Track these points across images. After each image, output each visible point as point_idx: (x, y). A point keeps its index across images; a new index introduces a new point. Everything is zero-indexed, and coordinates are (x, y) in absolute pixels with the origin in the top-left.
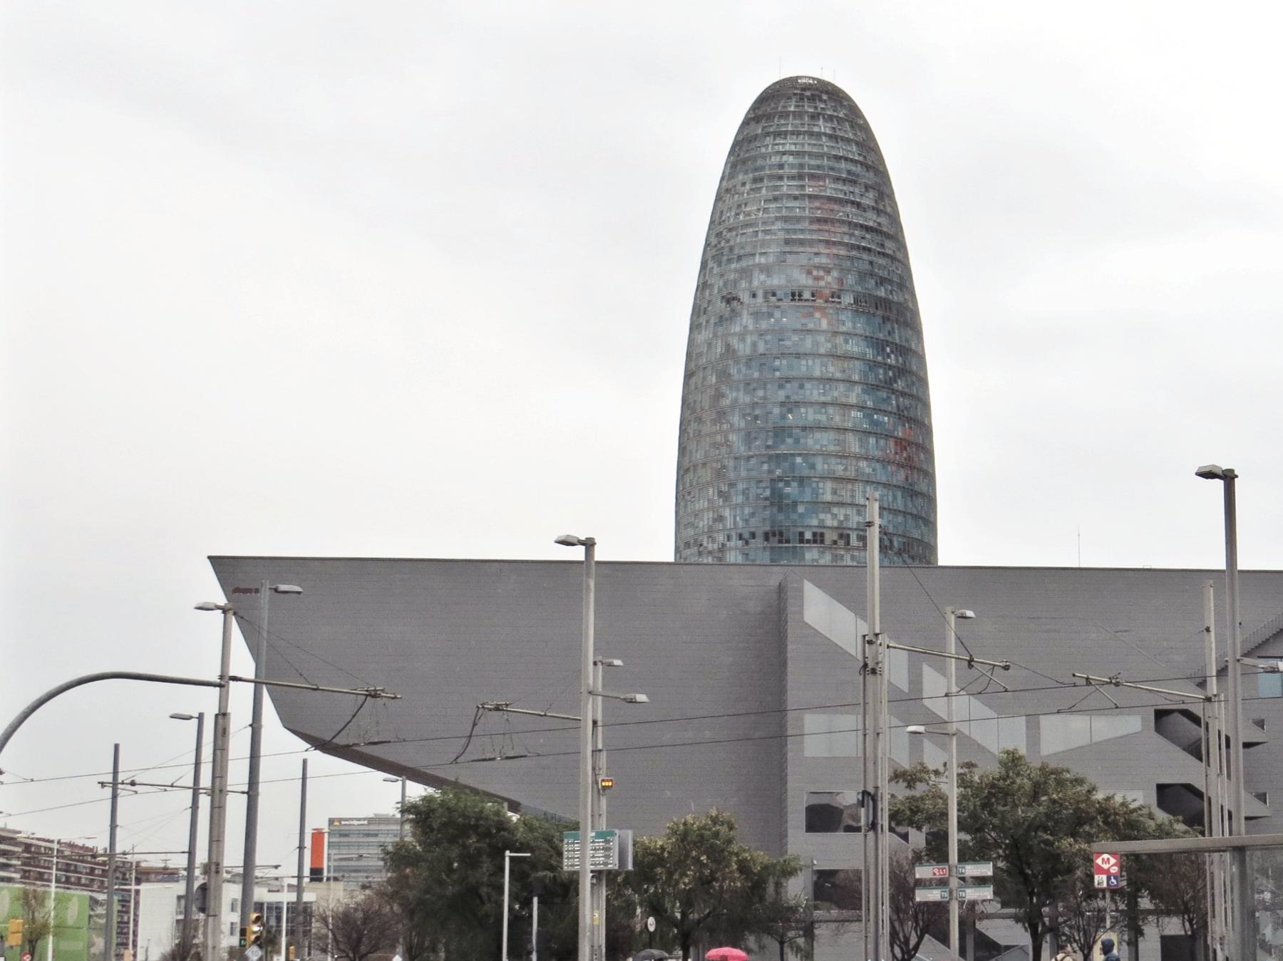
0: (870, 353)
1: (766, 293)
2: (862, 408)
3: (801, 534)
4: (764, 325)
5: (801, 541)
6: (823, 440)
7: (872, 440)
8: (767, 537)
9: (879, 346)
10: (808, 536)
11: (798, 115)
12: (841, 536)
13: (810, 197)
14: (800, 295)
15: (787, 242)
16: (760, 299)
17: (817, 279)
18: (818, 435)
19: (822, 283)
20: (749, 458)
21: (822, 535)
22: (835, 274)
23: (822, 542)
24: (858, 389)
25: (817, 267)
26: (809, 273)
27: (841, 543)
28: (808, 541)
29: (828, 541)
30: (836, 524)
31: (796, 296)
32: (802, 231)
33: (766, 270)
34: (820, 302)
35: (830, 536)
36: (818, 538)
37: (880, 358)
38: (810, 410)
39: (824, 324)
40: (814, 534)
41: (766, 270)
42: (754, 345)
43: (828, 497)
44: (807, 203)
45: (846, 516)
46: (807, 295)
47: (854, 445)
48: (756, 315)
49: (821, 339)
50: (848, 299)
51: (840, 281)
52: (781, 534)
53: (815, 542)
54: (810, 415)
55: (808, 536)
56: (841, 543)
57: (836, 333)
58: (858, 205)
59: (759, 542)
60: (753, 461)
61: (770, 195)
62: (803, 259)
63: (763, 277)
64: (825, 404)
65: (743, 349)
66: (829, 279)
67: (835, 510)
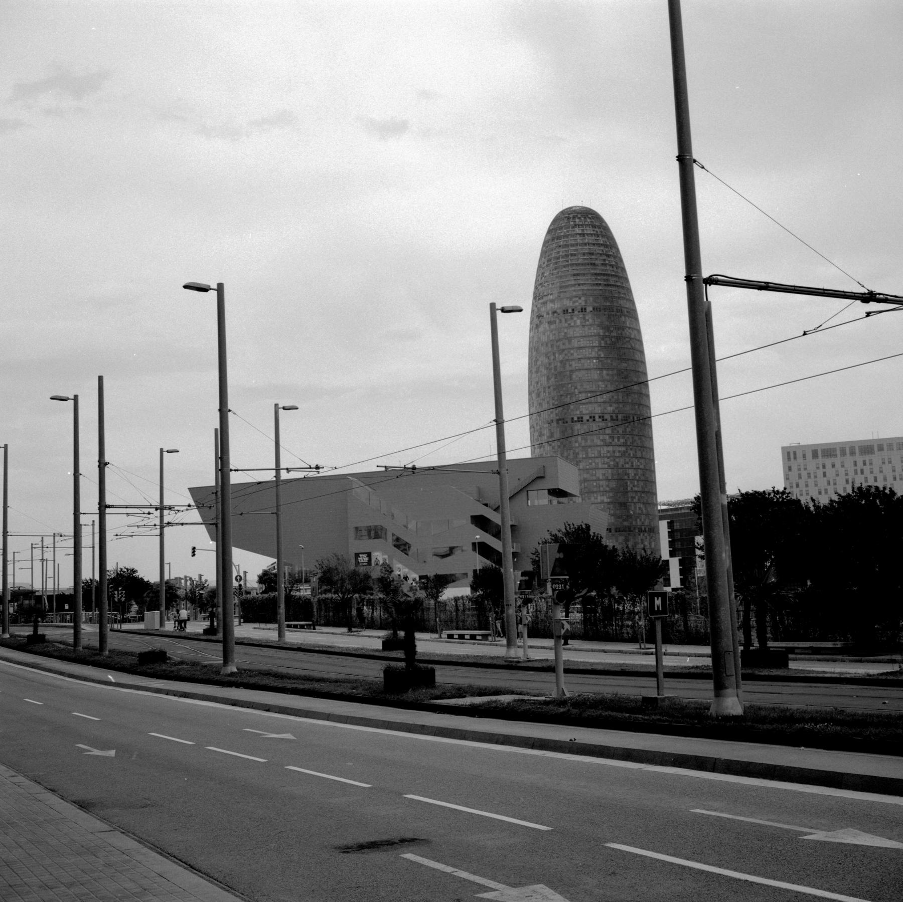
0: (601, 332)
2: (597, 358)
4: (553, 327)
6: (580, 374)
7: (605, 372)
8: (558, 420)
9: (607, 329)
10: (576, 419)
11: (567, 227)
13: (572, 265)
15: (561, 287)
16: (551, 315)
17: (574, 302)
18: (577, 373)
19: (577, 304)
20: (549, 387)
22: (583, 298)
24: (596, 349)
25: (576, 297)
26: (571, 300)
31: (565, 312)
33: (552, 301)
34: (576, 312)
35: (586, 418)
36: (580, 420)
37: (607, 334)
38: (573, 363)
39: (578, 322)
41: (552, 301)
42: (549, 337)
44: (570, 268)
46: (570, 310)
47: (595, 375)
48: (550, 323)
49: (577, 329)
50: (589, 309)
51: (586, 301)
54: (574, 364)
55: (576, 419)
57: (584, 326)
58: (594, 264)
59: (555, 424)
60: (552, 388)
62: (568, 295)
64: (579, 359)
65: (544, 339)
66: (580, 301)
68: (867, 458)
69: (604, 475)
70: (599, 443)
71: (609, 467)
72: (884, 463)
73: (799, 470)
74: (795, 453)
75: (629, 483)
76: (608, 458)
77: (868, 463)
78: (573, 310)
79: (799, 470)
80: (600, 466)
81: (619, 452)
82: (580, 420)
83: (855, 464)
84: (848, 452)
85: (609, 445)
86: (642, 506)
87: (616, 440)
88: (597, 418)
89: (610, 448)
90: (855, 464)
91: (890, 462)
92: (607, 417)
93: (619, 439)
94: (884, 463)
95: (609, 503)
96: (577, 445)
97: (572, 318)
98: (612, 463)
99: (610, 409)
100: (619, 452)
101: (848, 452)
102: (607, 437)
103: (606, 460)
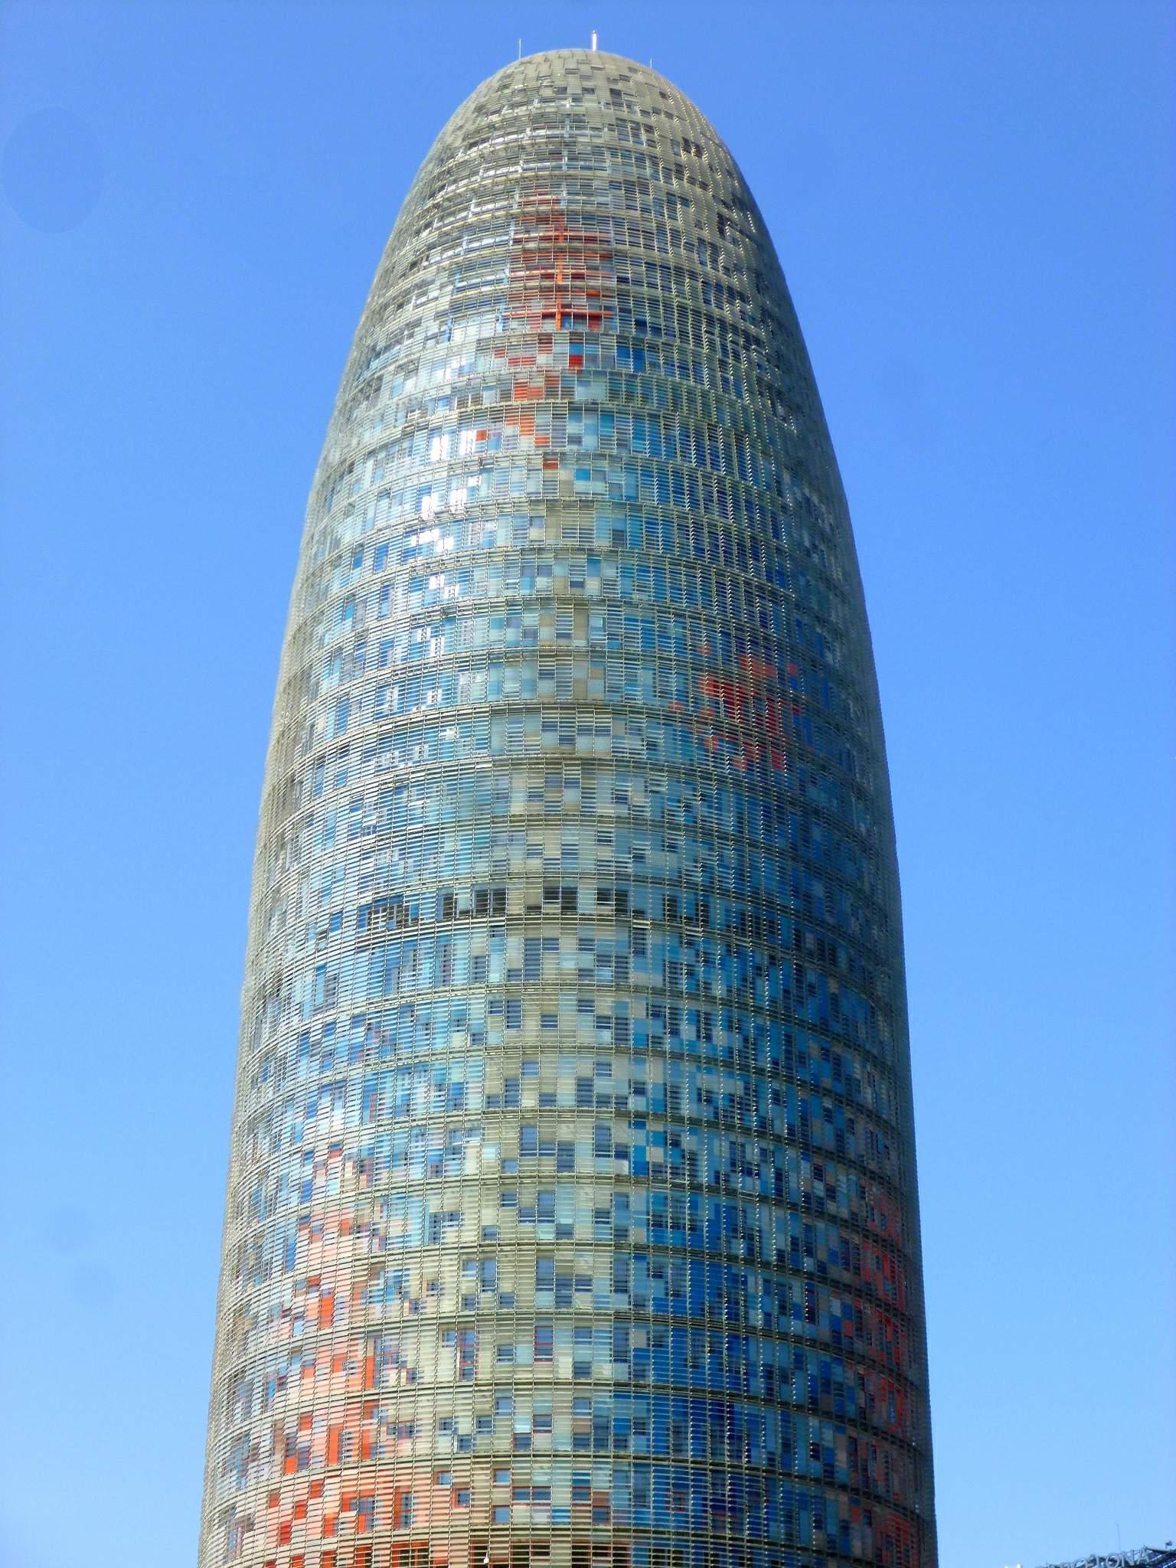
3: (448, 902)
5: (448, 915)
8: (365, 914)
10: (465, 899)
12: (550, 894)
14: (477, 400)
21: (500, 896)
23: (500, 909)
27: (554, 908)
28: (465, 913)
29: (515, 906)
30: (535, 864)
39: (526, 443)
40: (481, 896)
43: (518, 806)
45: (569, 852)
53: (482, 910)
56: (554, 908)
59: (349, 932)
66: (542, 359)
67: (535, 838)
69: (600, 1215)
70: (586, 1032)
75: (756, 1285)
76: (639, 1121)
80: (585, 1163)
81: (705, 1097)
82: (490, 901)
86: (828, 1435)
87: (687, 1031)
88: (586, 901)
89: (653, 1073)
93: (704, 1024)
95: (620, 1389)
96: (459, 1040)
98: (656, 1155)
102: (637, 1011)
103: (623, 1134)
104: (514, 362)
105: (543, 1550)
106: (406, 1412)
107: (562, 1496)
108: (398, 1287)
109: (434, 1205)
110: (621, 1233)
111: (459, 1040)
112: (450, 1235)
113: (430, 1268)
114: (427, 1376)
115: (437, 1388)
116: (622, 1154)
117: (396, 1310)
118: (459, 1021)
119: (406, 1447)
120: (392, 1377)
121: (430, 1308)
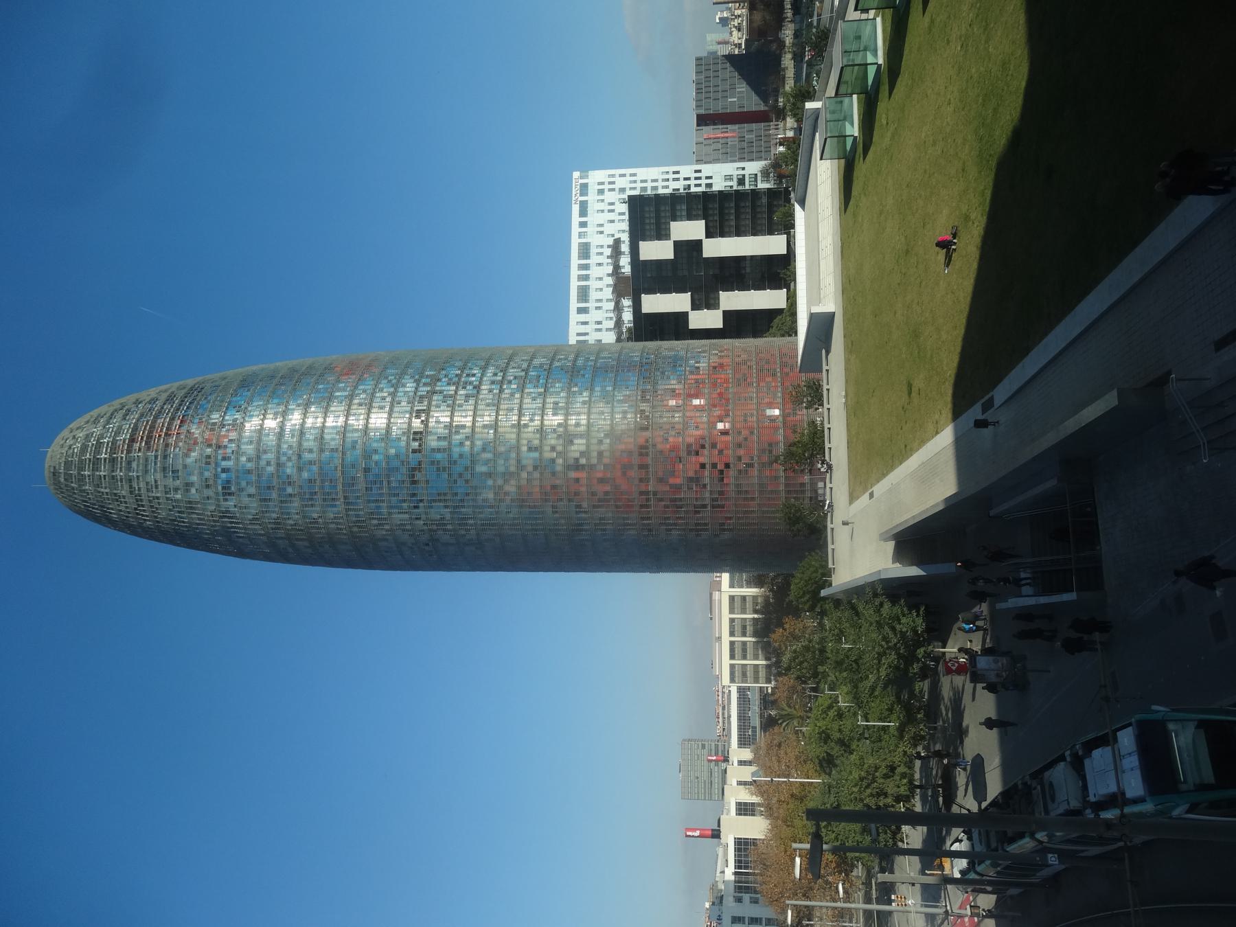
1: (208, 486)
3: (414, 451)
10: (416, 445)
12: (418, 417)
14: (209, 457)
16: (210, 492)
17: (196, 443)
19: (200, 440)
21: (415, 433)
23: (421, 433)
26: (189, 450)
32: (156, 457)
40: (414, 440)
52: (414, 469)
55: (416, 445)
61: (126, 487)
63: (193, 491)
68: (593, 250)
71: (522, 389)
72: (602, 233)
73: (600, 330)
74: (579, 334)
76: (501, 390)
77: (600, 250)
78: (210, 446)
79: (600, 330)
83: (600, 264)
84: (584, 272)
85: (477, 388)
90: (600, 264)
91: (602, 225)
92: (423, 390)
94: (602, 233)
97: (226, 447)
99: (410, 386)
100: (495, 375)
101: (584, 272)
104: (196, 443)
105: (643, 412)
106: (595, 454)
107: (625, 407)
108: (553, 461)
109: (525, 449)
110: (540, 394)
111: (468, 443)
112: (536, 442)
113: (547, 448)
114: (583, 448)
115: (588, 446)
116: (512, 395)
117: (560, 461)
118: (461, 444)
119: (607, 454)
120: (583, 461)
121: (560, 448)
